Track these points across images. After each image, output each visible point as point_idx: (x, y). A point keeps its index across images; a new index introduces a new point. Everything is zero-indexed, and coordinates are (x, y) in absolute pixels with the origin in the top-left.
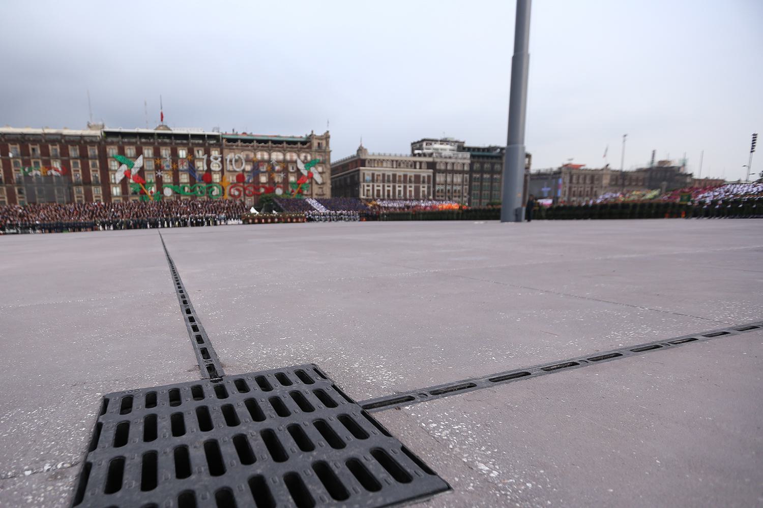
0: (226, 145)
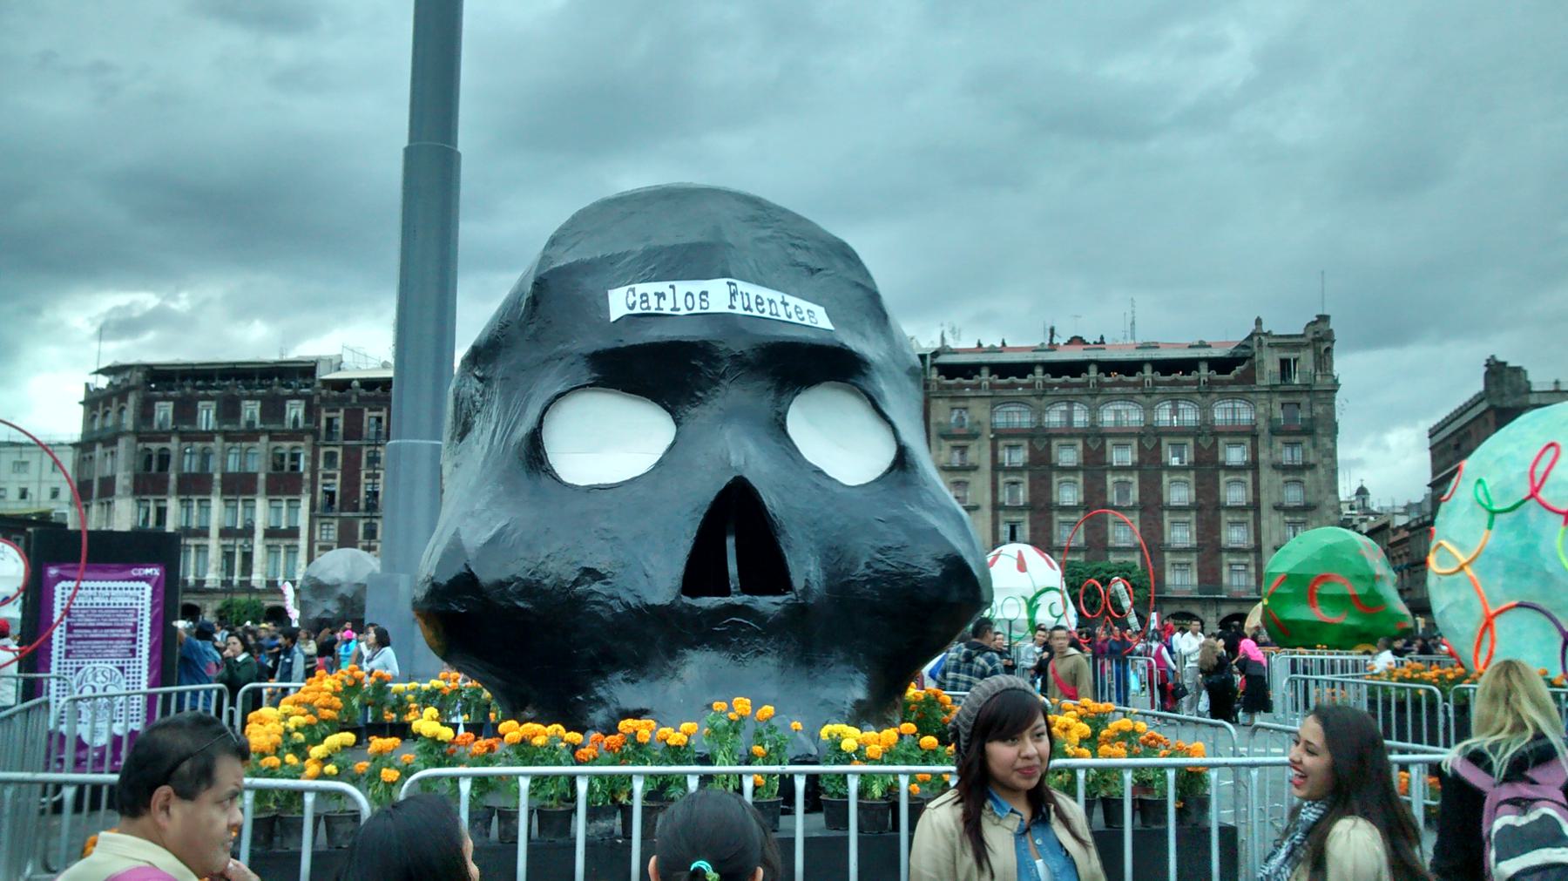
0: (941, 387)
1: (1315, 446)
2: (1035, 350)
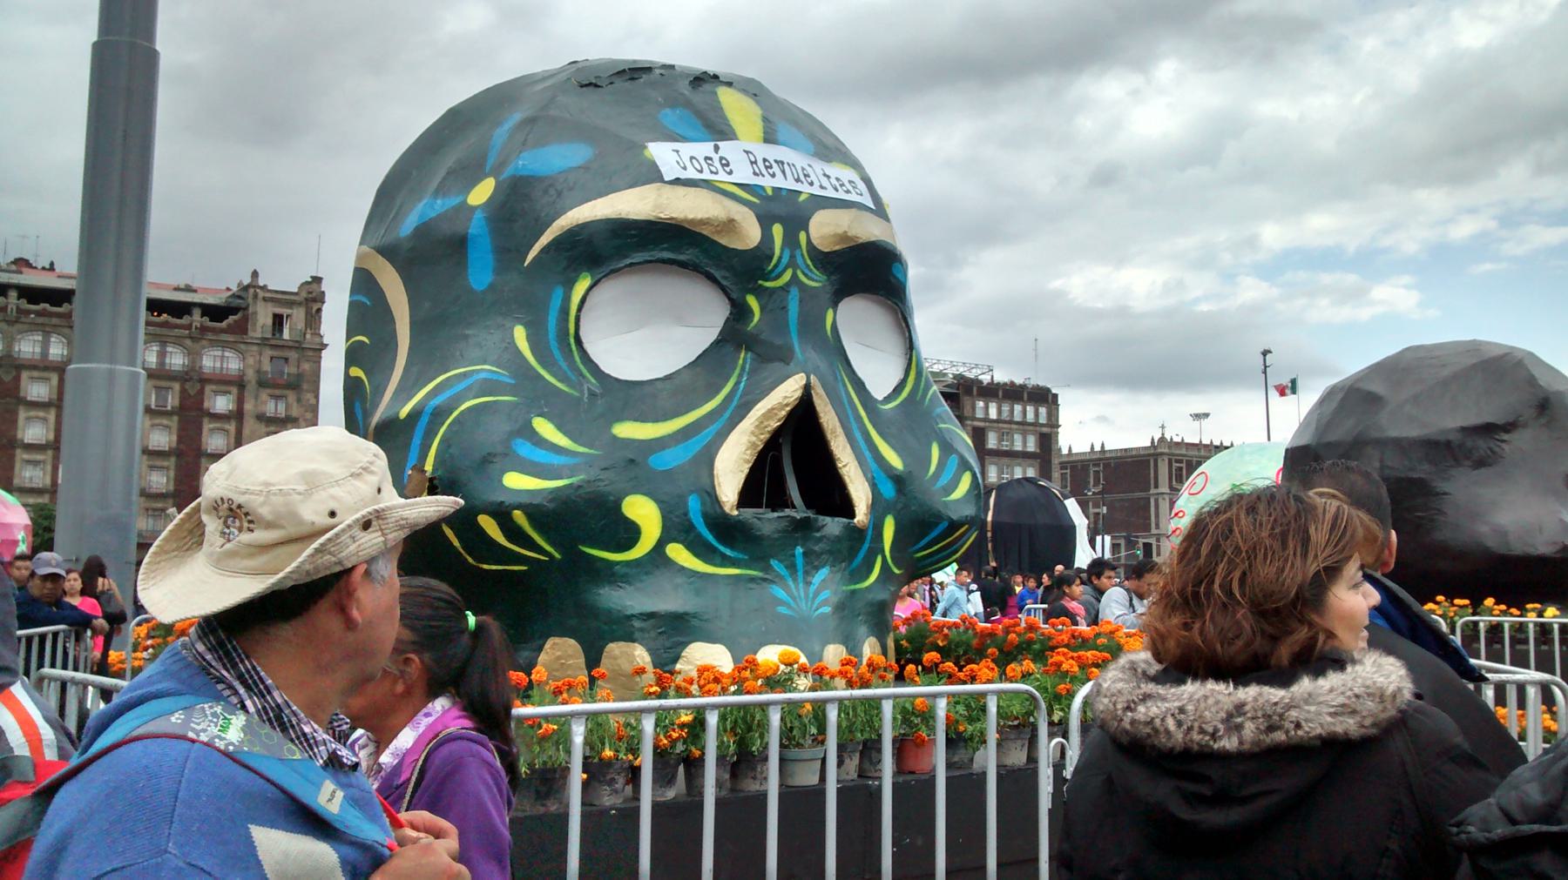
1: (299, 400)
2: (177, 289)
